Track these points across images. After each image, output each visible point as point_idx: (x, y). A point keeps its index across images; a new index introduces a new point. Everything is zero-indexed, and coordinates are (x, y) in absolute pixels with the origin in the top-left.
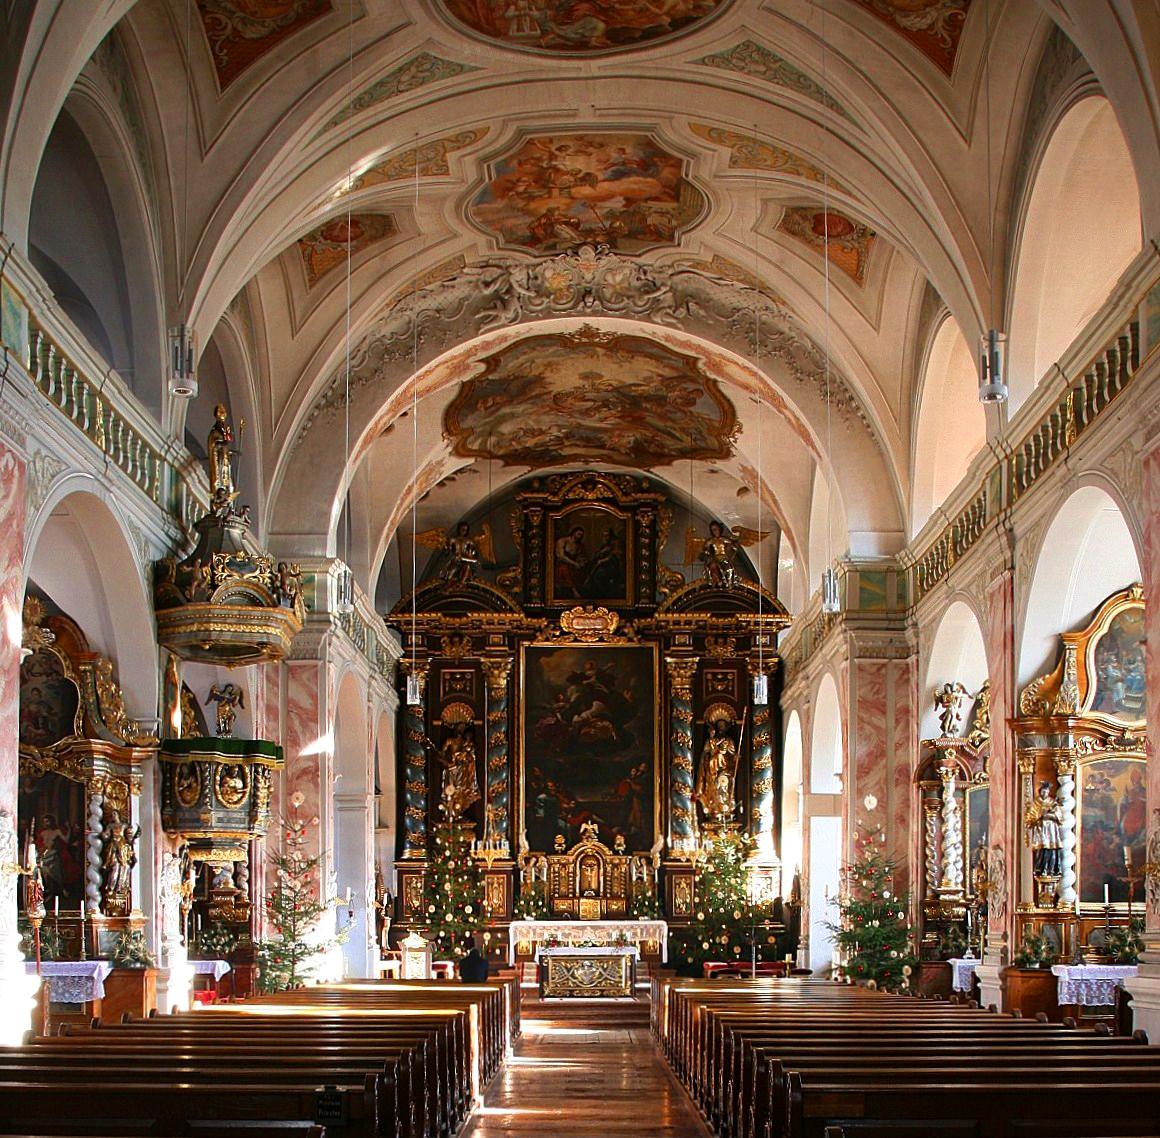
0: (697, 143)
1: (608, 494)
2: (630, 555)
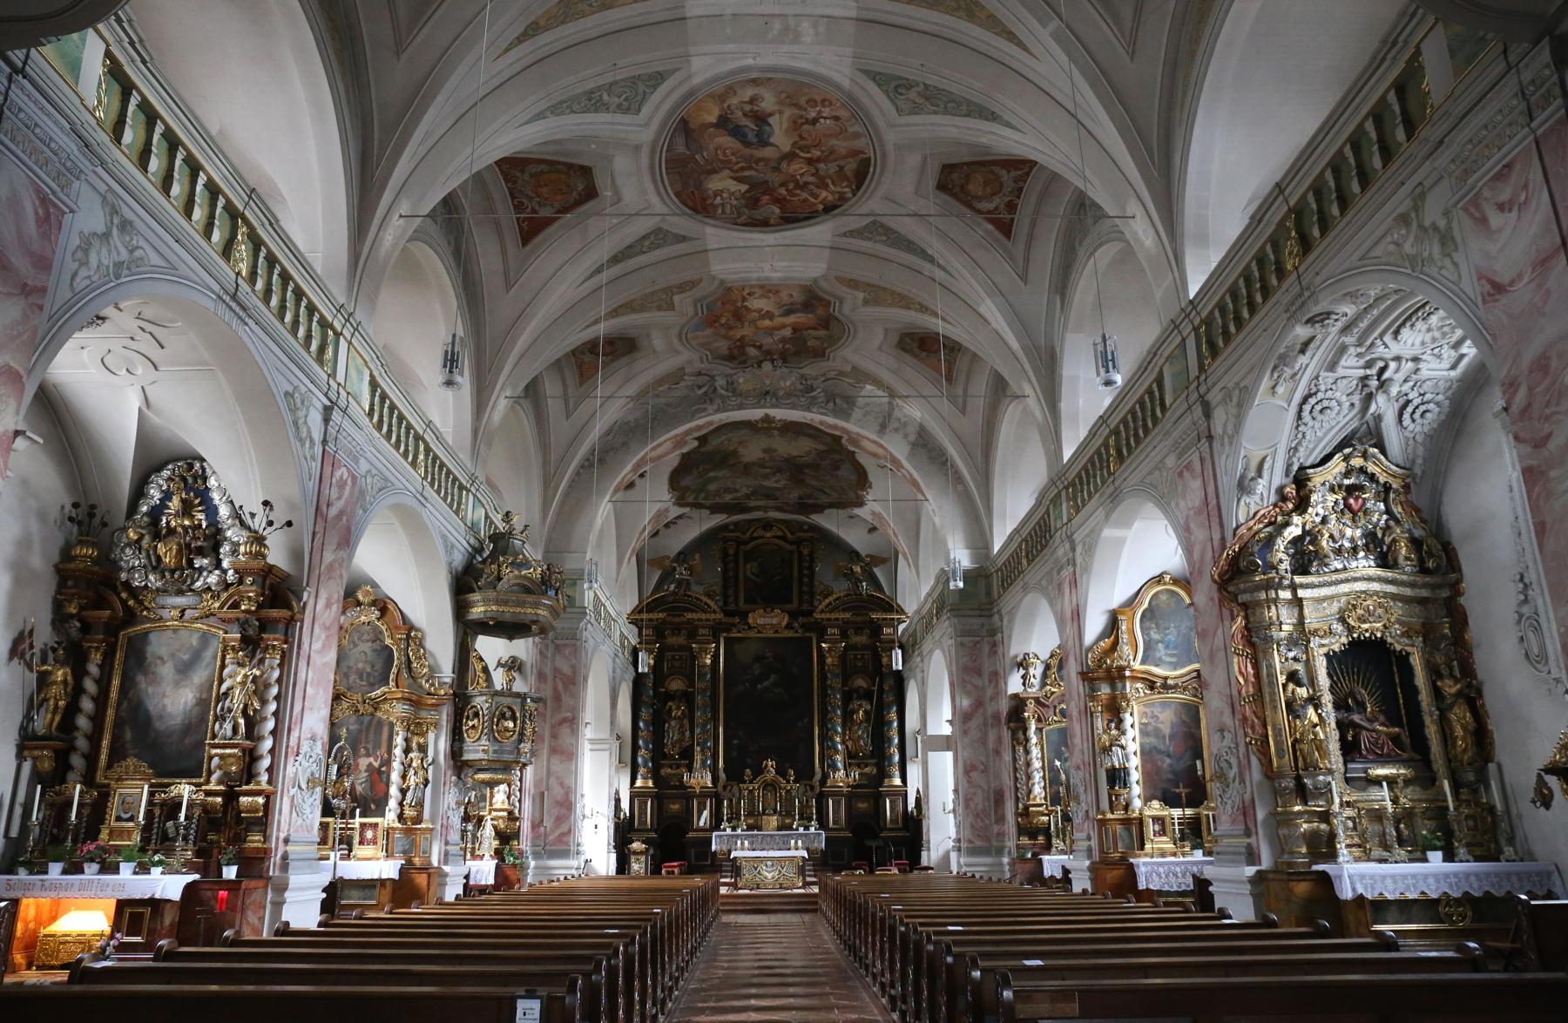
0: (842, 290)
1: (780, 534)
2: (796, 574)
